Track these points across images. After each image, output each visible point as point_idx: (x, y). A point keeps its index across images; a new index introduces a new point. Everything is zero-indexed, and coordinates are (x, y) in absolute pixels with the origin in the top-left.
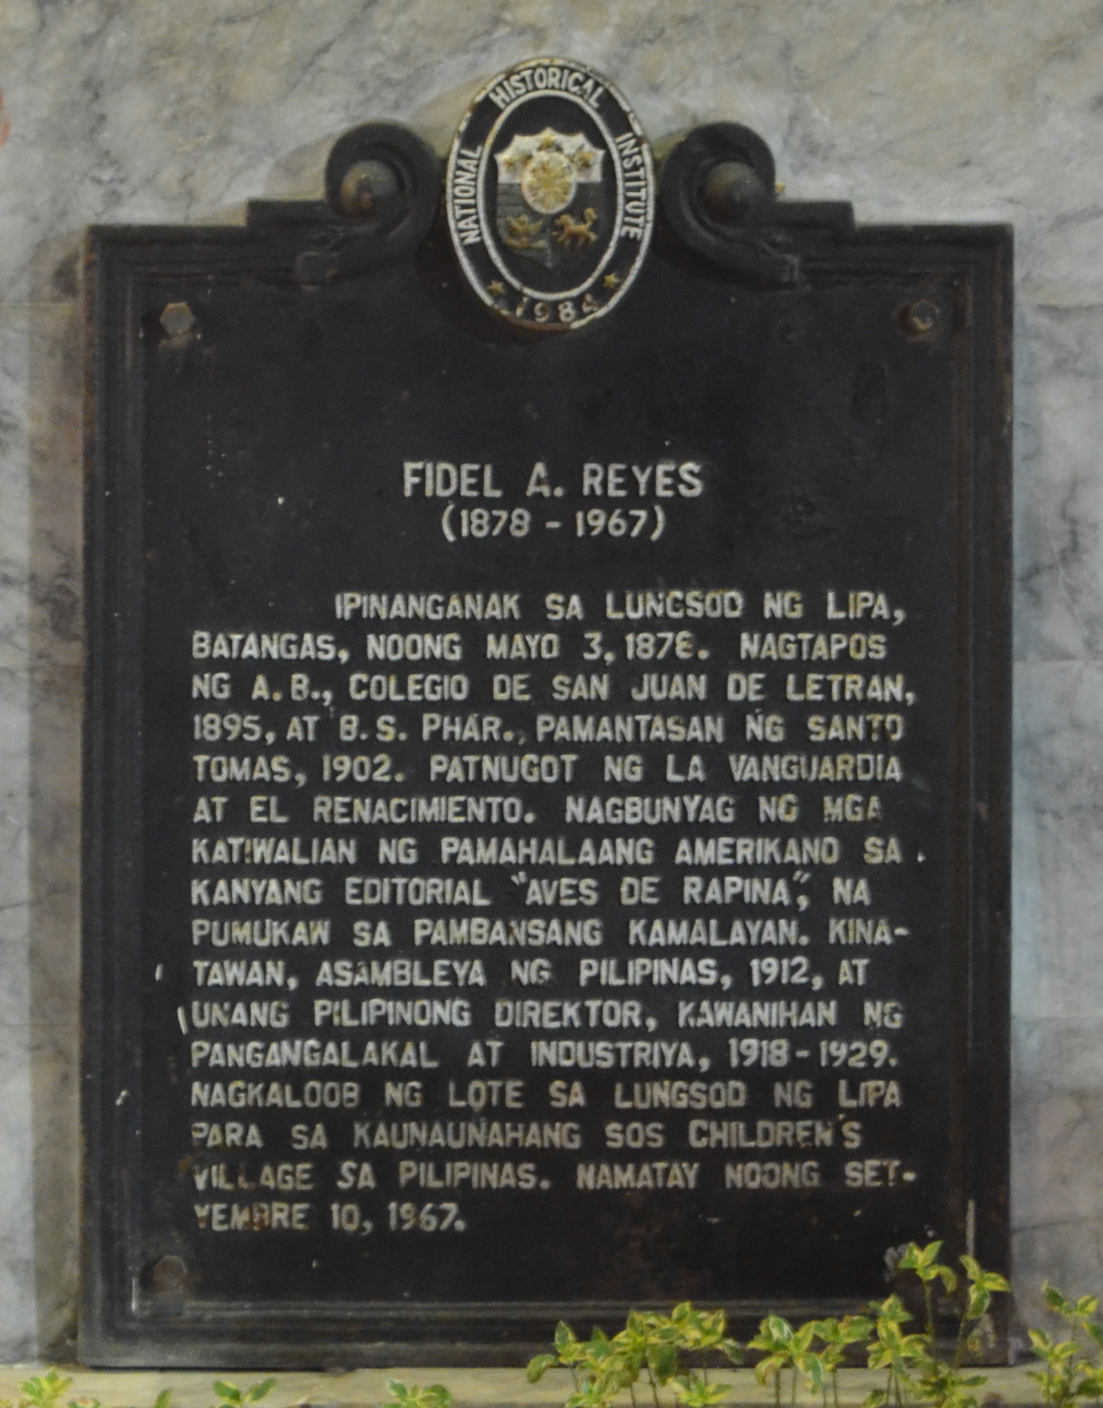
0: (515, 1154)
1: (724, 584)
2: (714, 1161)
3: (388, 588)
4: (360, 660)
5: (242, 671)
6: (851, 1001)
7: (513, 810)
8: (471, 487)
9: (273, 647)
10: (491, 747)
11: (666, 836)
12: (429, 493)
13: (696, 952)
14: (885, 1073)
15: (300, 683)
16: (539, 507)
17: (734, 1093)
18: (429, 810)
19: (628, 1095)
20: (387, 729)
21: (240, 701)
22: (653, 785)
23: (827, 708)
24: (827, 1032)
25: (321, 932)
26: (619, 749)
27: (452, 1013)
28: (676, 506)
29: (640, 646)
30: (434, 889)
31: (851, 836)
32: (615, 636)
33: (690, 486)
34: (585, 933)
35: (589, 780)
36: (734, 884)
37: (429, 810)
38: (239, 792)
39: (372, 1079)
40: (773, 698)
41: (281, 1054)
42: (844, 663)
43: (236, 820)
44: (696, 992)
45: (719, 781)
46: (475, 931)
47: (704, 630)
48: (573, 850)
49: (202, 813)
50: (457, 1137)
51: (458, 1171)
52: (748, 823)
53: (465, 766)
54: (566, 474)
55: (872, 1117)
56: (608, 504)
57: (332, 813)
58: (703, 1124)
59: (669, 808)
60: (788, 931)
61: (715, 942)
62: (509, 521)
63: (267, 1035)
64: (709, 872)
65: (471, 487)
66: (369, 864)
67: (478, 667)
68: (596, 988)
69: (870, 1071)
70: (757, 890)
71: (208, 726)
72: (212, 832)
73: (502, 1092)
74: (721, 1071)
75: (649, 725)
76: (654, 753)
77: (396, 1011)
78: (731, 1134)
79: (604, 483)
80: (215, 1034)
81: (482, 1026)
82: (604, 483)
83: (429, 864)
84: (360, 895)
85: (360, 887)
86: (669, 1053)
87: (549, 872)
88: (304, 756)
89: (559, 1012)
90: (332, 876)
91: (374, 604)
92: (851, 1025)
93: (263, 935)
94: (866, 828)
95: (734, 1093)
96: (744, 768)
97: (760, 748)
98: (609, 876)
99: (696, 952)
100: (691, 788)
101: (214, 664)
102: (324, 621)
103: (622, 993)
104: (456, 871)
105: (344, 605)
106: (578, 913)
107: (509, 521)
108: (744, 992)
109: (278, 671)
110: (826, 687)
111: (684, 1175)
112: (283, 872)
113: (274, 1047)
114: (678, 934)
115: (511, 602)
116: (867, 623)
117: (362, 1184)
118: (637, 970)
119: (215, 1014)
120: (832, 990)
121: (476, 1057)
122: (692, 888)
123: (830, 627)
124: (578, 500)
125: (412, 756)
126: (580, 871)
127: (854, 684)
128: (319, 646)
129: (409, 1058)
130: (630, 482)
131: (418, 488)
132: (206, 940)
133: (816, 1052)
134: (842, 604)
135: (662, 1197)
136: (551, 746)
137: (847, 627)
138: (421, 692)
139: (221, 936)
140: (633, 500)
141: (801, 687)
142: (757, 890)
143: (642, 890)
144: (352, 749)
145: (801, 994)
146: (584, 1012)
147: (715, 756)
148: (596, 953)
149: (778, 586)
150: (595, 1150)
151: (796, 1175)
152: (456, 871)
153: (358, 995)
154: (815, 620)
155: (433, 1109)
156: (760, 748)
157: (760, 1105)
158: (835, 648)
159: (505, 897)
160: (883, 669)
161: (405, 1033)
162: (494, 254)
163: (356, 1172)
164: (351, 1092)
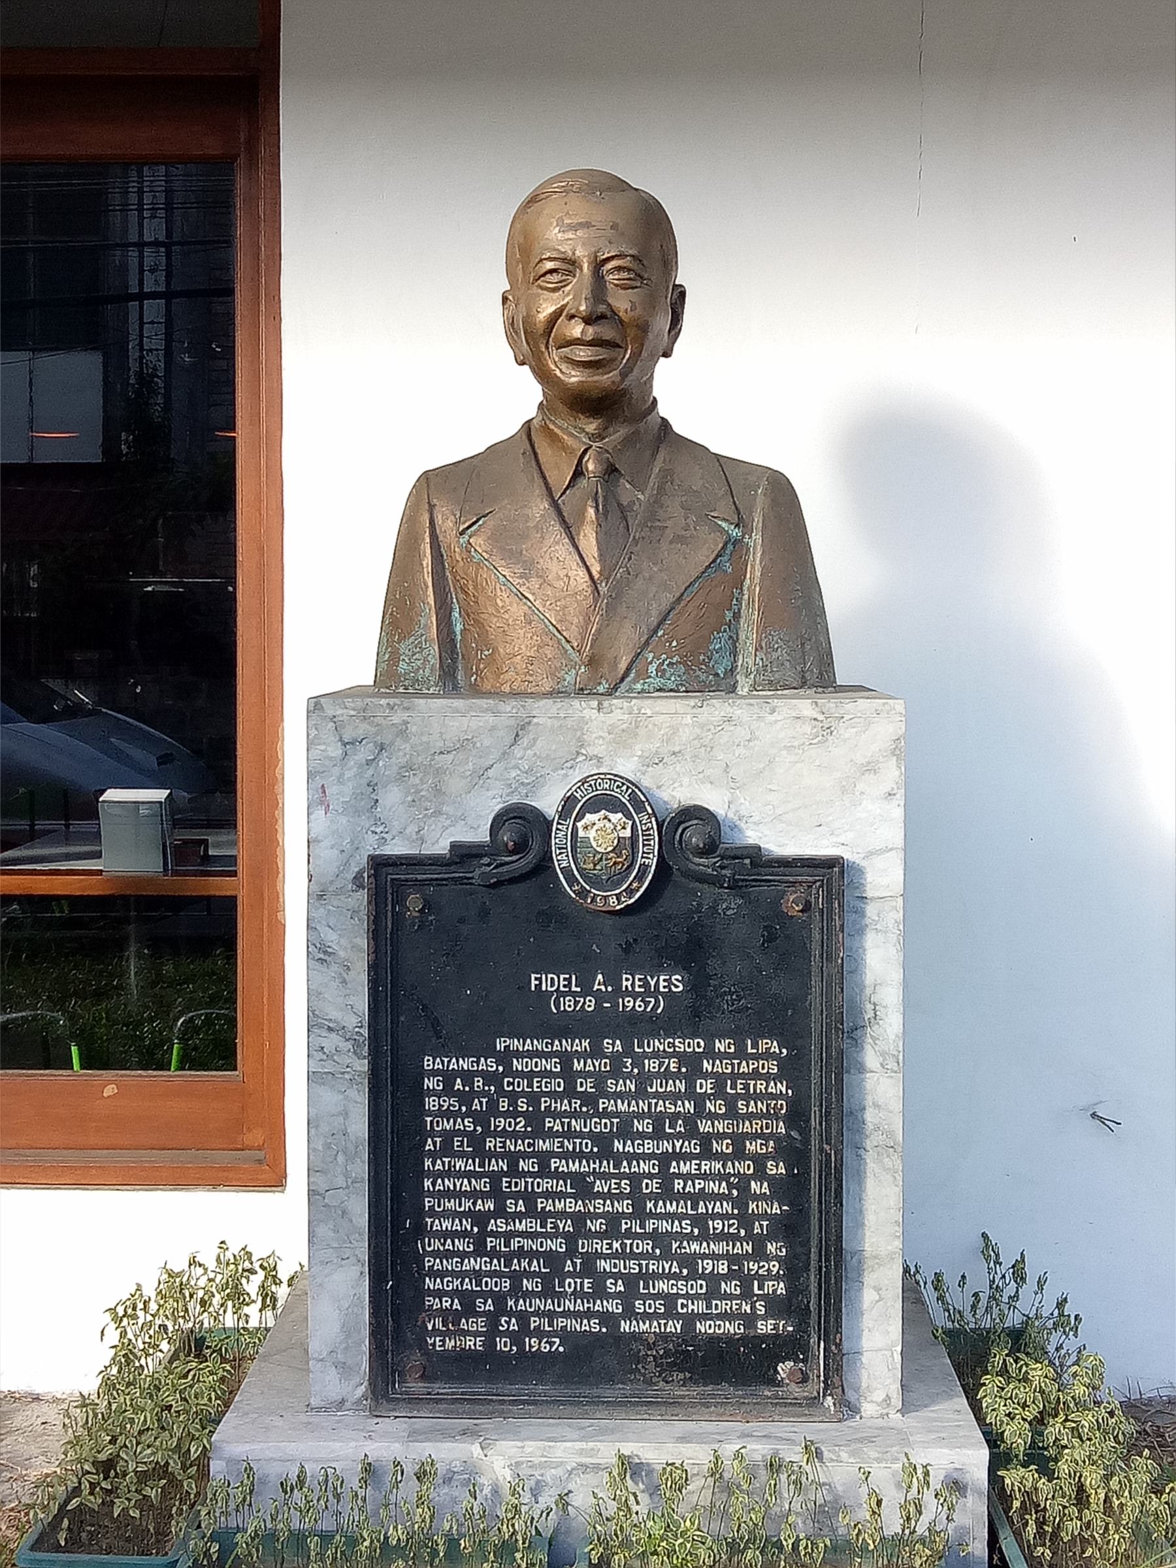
0: (589, 1314)
1: (693, 1036)
2: (690, 1320)
3: (522, 1036)
4: (509, 1071)
5: (448, 1077)
6: (760, 1243)
7: (588, 1146)
8: (565, 986)
9: (465, 1064)
10: (574, 1115)
11: (665, 1160)
12: (544, 988)
13: (681, 1217)
14: (777, 1278)
15: (479, 1083)
16: (600, 997)
17: (701, 1287)
18: (543, 1145)
19: (646, 1287)
20: (522, 1105)
21: (448, 1090)
22: (658, 1134)
23: (747, 1097)
24: (747, 1257)
25: (490, 1205)
26: (640, 1116)
27: (557, 1245)
28: (670, 996)
29: (651, 1065)
30: (547, 1184)
31: (759, 1161)
32: (638, 1062)
33: (677, 987)
34: (624, 1206)
35: (625, 1131)
36: (699, 1184)
37: (543, 1145)
38: (448, 1136)
39: (516, 1278)
40: (719, 1092)
41: (470, 1264)
42: (756, 1075)
43: (446, 1149)
44: (681, 1236)
45: (692, 1132)
46: (572, 1206)
47: (682, 1058)
48: (617, 1166)
49: (429, 1146)
50: (559, 1306)
51: (561, 1322)
52: (707, 1153)
53: (563, 1124)
54: (613, 979)
55: (768, 1299)
56: (635, 996)
57: (495, 1146)
58: (685, 1302)
59: (666, 1146)
60: (727, 1207)
61: (690, 1212)
62: (584, 1003)
63: (463, 1255)
64: (687, 1177)
65: (565, 986)
66: (514, 1171)
67: (568, 1074)
68: (629, 1234)
69: (769, 1276)
70: (713, 1187)
71: (431, 1103)
72: (434, 1155)
73: (582, 1284)
74: (694, 1275)
75: (656, 1104)
76: (658, 1120)
77: (527, 1244)
78: (699, 1307)
79: (633, 985)
80: (436, 1254)
81: (572, 1252)
82: (633, 985)
83: (544, 1171)
84: (510, 1187)
85: (510, 1183)
86: (667, 1266)
87: (606, 1177)
88: (480, 1118)
89: (610, 1246)
90: (495, 1178)
91: (515, 1044)
92: (760, 1254)
93: (460, 1206)
94: (766, 1157)
95: (701, 1287)
96: (704, 1127)
97: (713, 1116)
98: (635, 1179)
99: (681, 1217)
100: (679, 1136)
101: (434, 1073)
102: (489, 1051)
103: (642, 1237)
104: (558, 1175)
105: (500, 1045)
106: (620, 1197)
107: (584, 1003)
108: (704, 1236)
109: (467, 1077)
110: (746, 1087)
111: (674, 1327)
112: (469, 1175)
113: (466, 1261)
114: (671, 1208)
115: (585, 1043)
116: (767, 1056)
117: (511, 1328)
118: (650, 1225)
119: (436, 1244)
120: (750, 1236)
121: (569, 1267)
122: (678, 1185)
123: (748, 1057)
124: (619, 992)
125: (535, 1119)
126: (621, 1176)
127: (761, 1086)
128: (489, 1065)
129: (535, 1266)
130: (646, 985)
131: (538, 986)
132: (432, 1208)
133: (741, 1266)
134: (755, 1045)
135: (664, 1337)
136: (605, 1114)
137: (756, 1057)
138: (540, 1087)
139: (439, 1206)
140: (647, 992)
141: (734, 1087)
142: (713, 1187)
143: (653, 1186)
144: (506, 1115)
145: (734, 1238)
146: (623, 1245)
147: (690, 1122)
148: (630, 1217)
149: (722, 1037)
150: (629, 1313)
151: (731, 1328)
152: (558, 1175)
153: (509, 1236)
154: (741, 1054)
155: (548, 1292)
156: (713, 1116)
157: (713, 1293)
158: (751, 1067)
159: (582, 1187)
160: (777, 1078)
161: (532, 1255)
162: (576, 872)
163: (508, 1323)
164: (506, 1284)
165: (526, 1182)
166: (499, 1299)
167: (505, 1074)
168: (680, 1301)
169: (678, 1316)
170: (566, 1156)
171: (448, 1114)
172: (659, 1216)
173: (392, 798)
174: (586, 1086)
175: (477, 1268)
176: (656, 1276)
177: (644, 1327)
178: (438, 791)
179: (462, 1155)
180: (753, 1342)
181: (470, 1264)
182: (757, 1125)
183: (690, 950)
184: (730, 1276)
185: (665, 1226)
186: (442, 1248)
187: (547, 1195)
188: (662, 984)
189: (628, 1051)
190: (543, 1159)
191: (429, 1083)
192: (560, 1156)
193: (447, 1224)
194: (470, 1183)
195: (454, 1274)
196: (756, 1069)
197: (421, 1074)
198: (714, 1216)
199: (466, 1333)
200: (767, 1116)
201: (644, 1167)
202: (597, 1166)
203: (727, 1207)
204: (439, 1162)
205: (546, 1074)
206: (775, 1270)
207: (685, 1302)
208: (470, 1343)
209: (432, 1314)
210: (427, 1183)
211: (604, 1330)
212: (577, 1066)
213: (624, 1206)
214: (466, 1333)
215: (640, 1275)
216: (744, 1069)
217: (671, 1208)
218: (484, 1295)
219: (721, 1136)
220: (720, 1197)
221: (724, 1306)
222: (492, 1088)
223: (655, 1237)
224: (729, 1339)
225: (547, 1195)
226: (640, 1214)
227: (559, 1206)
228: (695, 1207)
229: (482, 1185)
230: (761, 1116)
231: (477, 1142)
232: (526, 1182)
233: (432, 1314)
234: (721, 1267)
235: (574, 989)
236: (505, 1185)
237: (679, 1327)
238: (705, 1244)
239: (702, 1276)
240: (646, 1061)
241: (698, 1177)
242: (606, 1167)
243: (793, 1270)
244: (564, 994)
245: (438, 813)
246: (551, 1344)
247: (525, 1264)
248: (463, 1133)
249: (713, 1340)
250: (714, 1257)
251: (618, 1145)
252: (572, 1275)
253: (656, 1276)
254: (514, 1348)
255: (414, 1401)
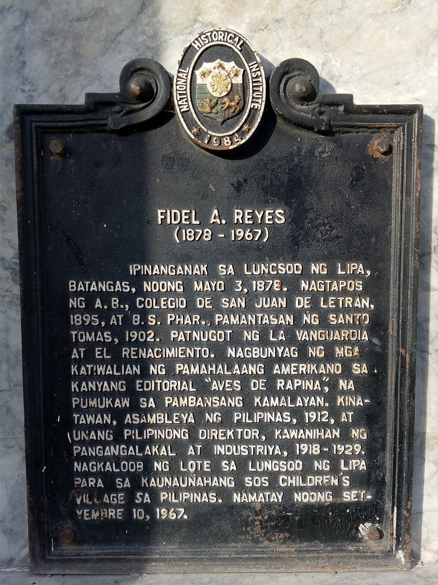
0: (207, 489)
1: (294, 260)
2: (289, 492)
4: (140, 292)
5: (90, 297)
9: (103, 287)
10: (195, 327)
11: (269, 363)
14: (359, 457)
15: (115, 302)
17: (297, 465)
18: (171, 353)
21: (90, 308)
22: (264, 342)
23: (337, 311)
24: (335, 440)
25: (126, 402)
26: (249, 327)
27: (181, 434)
28: (274, 227)
29: (258, 286)
30: (173, 384)
35: (236, 340)
36: (298, 383)
38: (90, 347)
40: (315, 307)
41: (110, 451)
42: (344, 292)
43: (89, 357)
44: (282, 425)
45: (292, 339)
46: (192, 401)
47: (284, 279)
48: (230, 368)
49: (75, 355)
52: (303, 357)
56: (244, 226)
57: (130, 354)
58: (285, 477)
59: (271, 352)
61: (289, 405)
62: (203, 234)
63: (104, 444)
64: (287, 377)
67: (189, 293)
68: (240, 423)
69: (354, 456)
70: (308, 385)
71: (76, 319)
72: (79, 363)
74: (292, 456)
78: (296, 481)
80: (82, 443)
81: (193, 439)
83: (171, 374)
84: (142, 387)
85: (142, 384)
86: (271, 450)
87: (220, 378)
88: (117, 331)
89: (225, 434)
90: (130, 380)
92: (346, 438)
93: (102, 404)
95: (297, 465)
96: (302, 335)
97: (308, 327)
98: (245, 379)
100: (280, 343)
101: (78, 294)
102: (124, 276)
104: (181, 377)
105: (133, 269)
106: (233, 394)
107: (203, 234)
108: (301, 425)
109: (106, 297)
110: (336, 303)
111: (276, 497)
112: (109, 378)
113: (108, 448)
114: (274, 402)
115: (204, 268)
116: (354, 276)
120: (338, 424)
121: (191, 451)
122: (280, 384)
123: (338, 278)
126: (234, 377)
127: (349, 301)
128: (124, 287)
129: (163, 451)
132: (78, 406)
133: (331, 449)
134: (344, 268)
135: (268, 506)
136: (220, 326)
137: (346, 277)
139: (84, 404)
142: (308, 385)
143: (258, 385)
144: (138, 328)
147: (290, 332)
148: (241, 410)
149: (316, 260)
150: (240, 487)
151: (324, 498)
152: (181, 377)
154: (332, 275)
155: (174, 472)
156: (308, 327)
158: (341, 286)
159: (202, 387)
160: (362, 295)
164: (140, 466)
165: (156, 384)
166: (135, 478)
167: (137, 294)
168: (281, 477)
169: (280, 489)
170: (188, 361)
171: (90, 328)
172: (264, 409)
173: (37, 60)
174: (203, 303)
175: (117, 454)
176: (261, 458)
177: (252, 498)
178: (76, 55)
179: (103, 362)
180: (339, 508)
181: (110, 451)
182: (345, 333)
183: (291, 188)
184: (321, 456)
185: (268, 417)
186: (87, 438)
187: (173, 393)
188: (267, 217)
189: (239, 274)
190: (170, 364)
191: (72, 303)
192: (184, 361)
193: (90, 419)
194: (109, 385)
195: (97, 458)
196: (343, 289)
197: (67, 295)
198: (310, 409)
199: (108, 506)
200: (354, 326)
201: (252, 369)
202: (214, 369)
203: (320, 401)
204: (83, 368)
205: (170, 293)
206: (358, 451)
207: (285, 477)
208: (111, 513)
209: (80, 491)
210: (74, 386)
211: (220, 501)
212: (197, 287)
213: (236, 402)
214: (108, 506)
215: (249, 457)
216: (335, 287)
217: (274, 402)
218: (122, 475)
219: (315, 344)
220: (315, 393)
221: (316, 480)
222: (127, 306)
223: (262, 426)
224: (321, 507)
225: (173, 393)
226: (249, 407)
227: (183, 402)
228: (293, 401)
229: (119, 386)
230: (347, 326)
231: (114, 351)
232: (156, 384)
233: (80, 491)
234: (315, 449)
235: (194, 222)
236: (138, 386)
237: (280, 497)
238: (302, 431)
239: (300, 457)
240: (254, 282)
241: (296, 376)
242: (221, 369)
243: (372, 450)
244: (186, 227)
245: (77, 73)
246: (177, 513)
247: (155, 449)
248: (103, 344)
249: (308, 507)
250: (309, 441)
251: (231, 352)
252: (195, 458)
253: (261, 458)
254: (148, 517)
255: (66, 561)
